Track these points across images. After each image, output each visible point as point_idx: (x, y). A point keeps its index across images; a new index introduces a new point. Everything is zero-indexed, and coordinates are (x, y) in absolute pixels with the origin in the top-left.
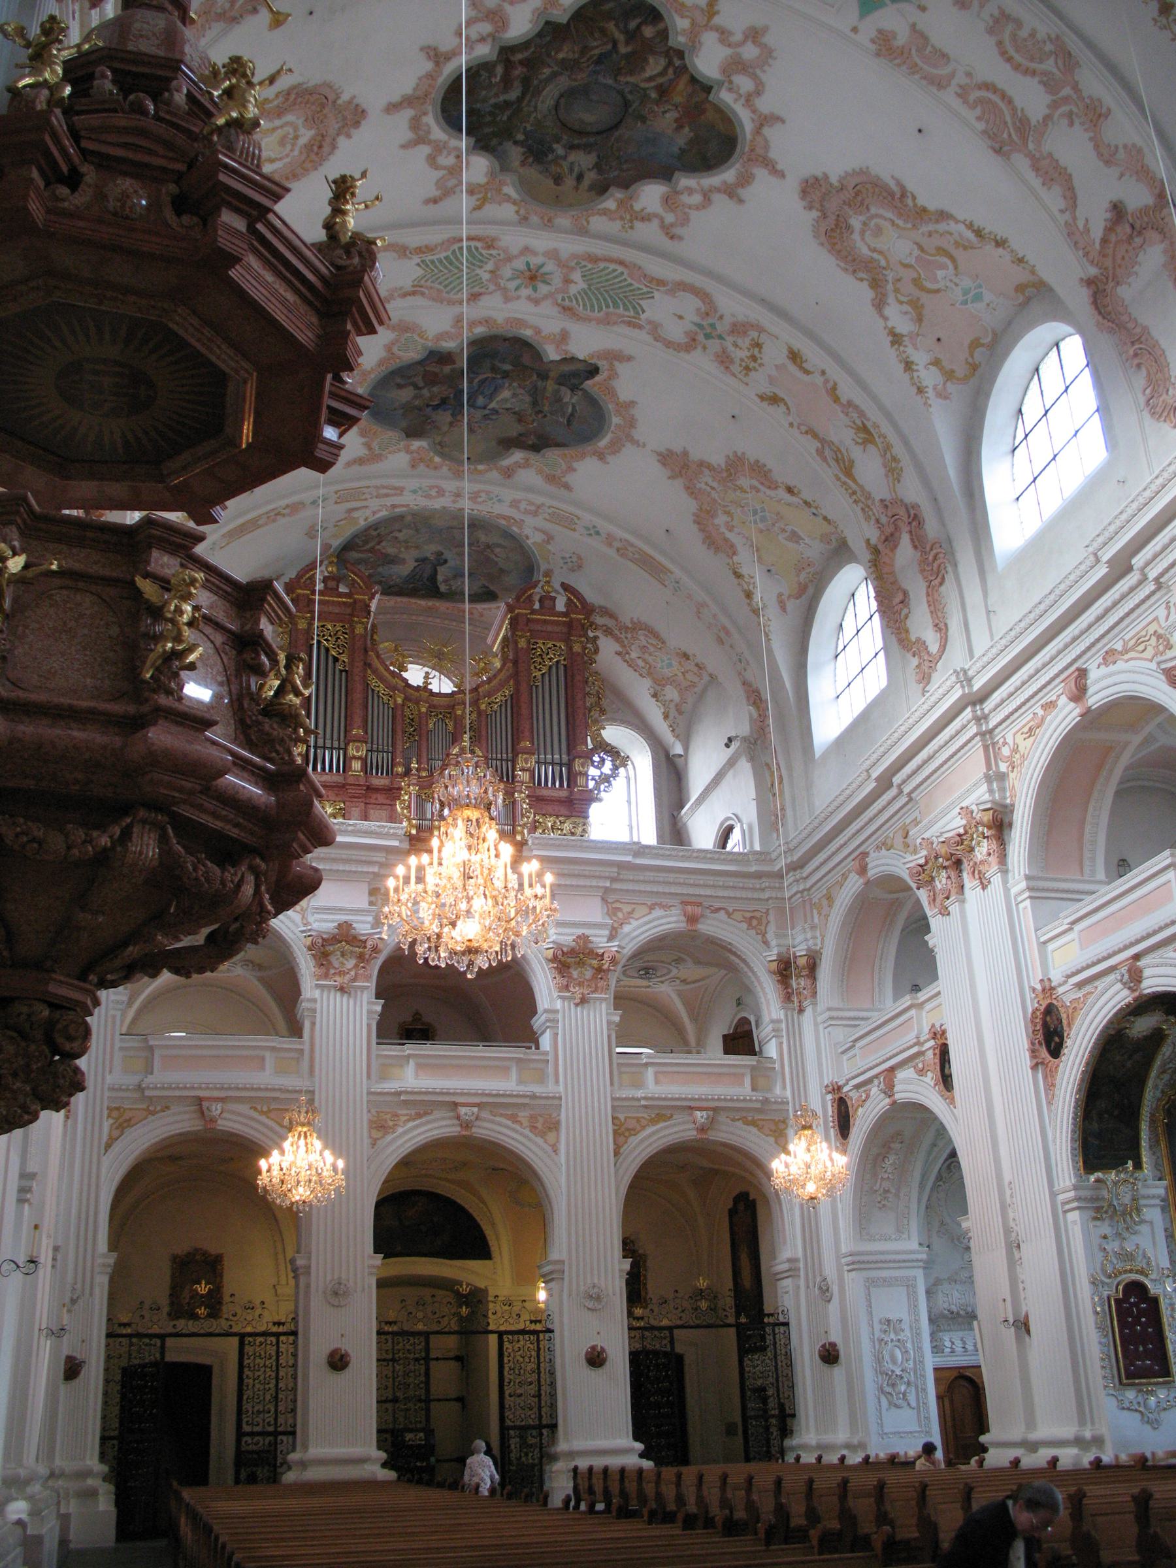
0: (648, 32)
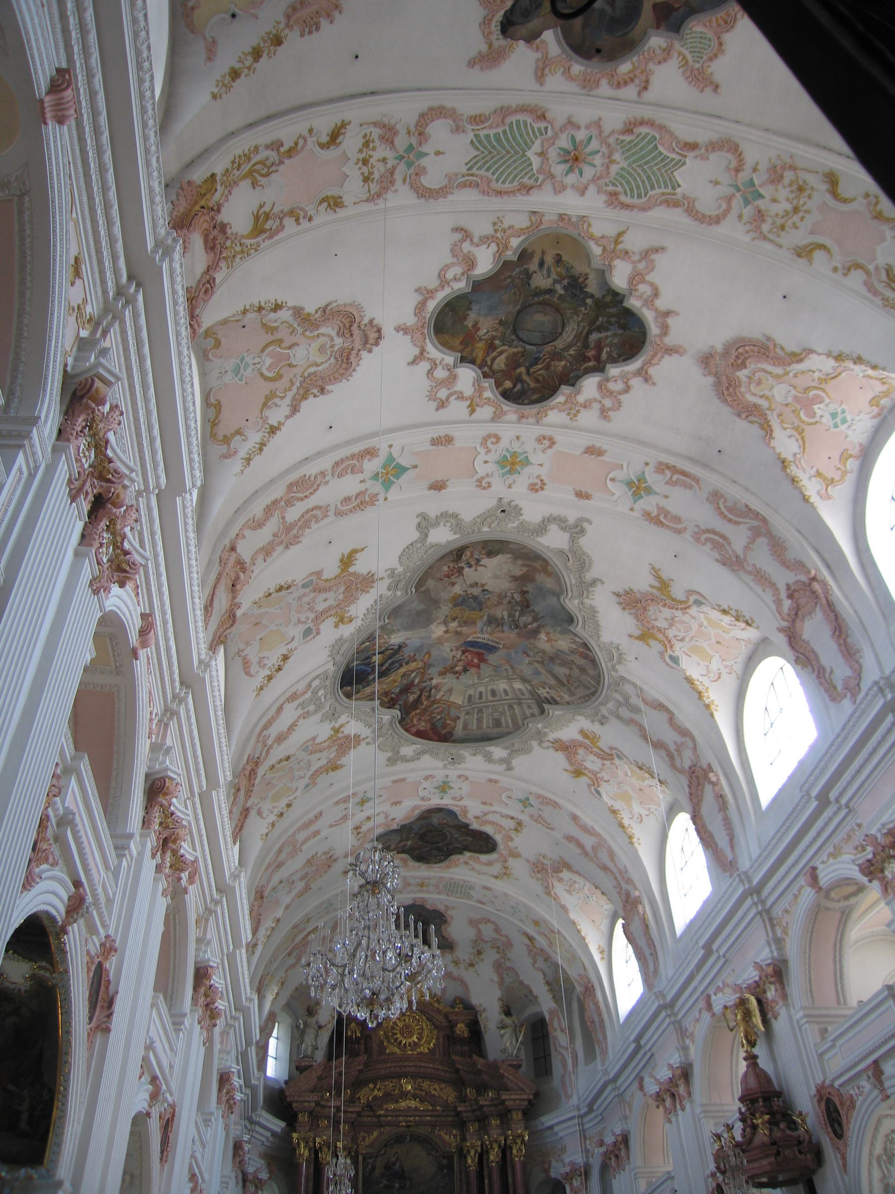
0: (508, 384)
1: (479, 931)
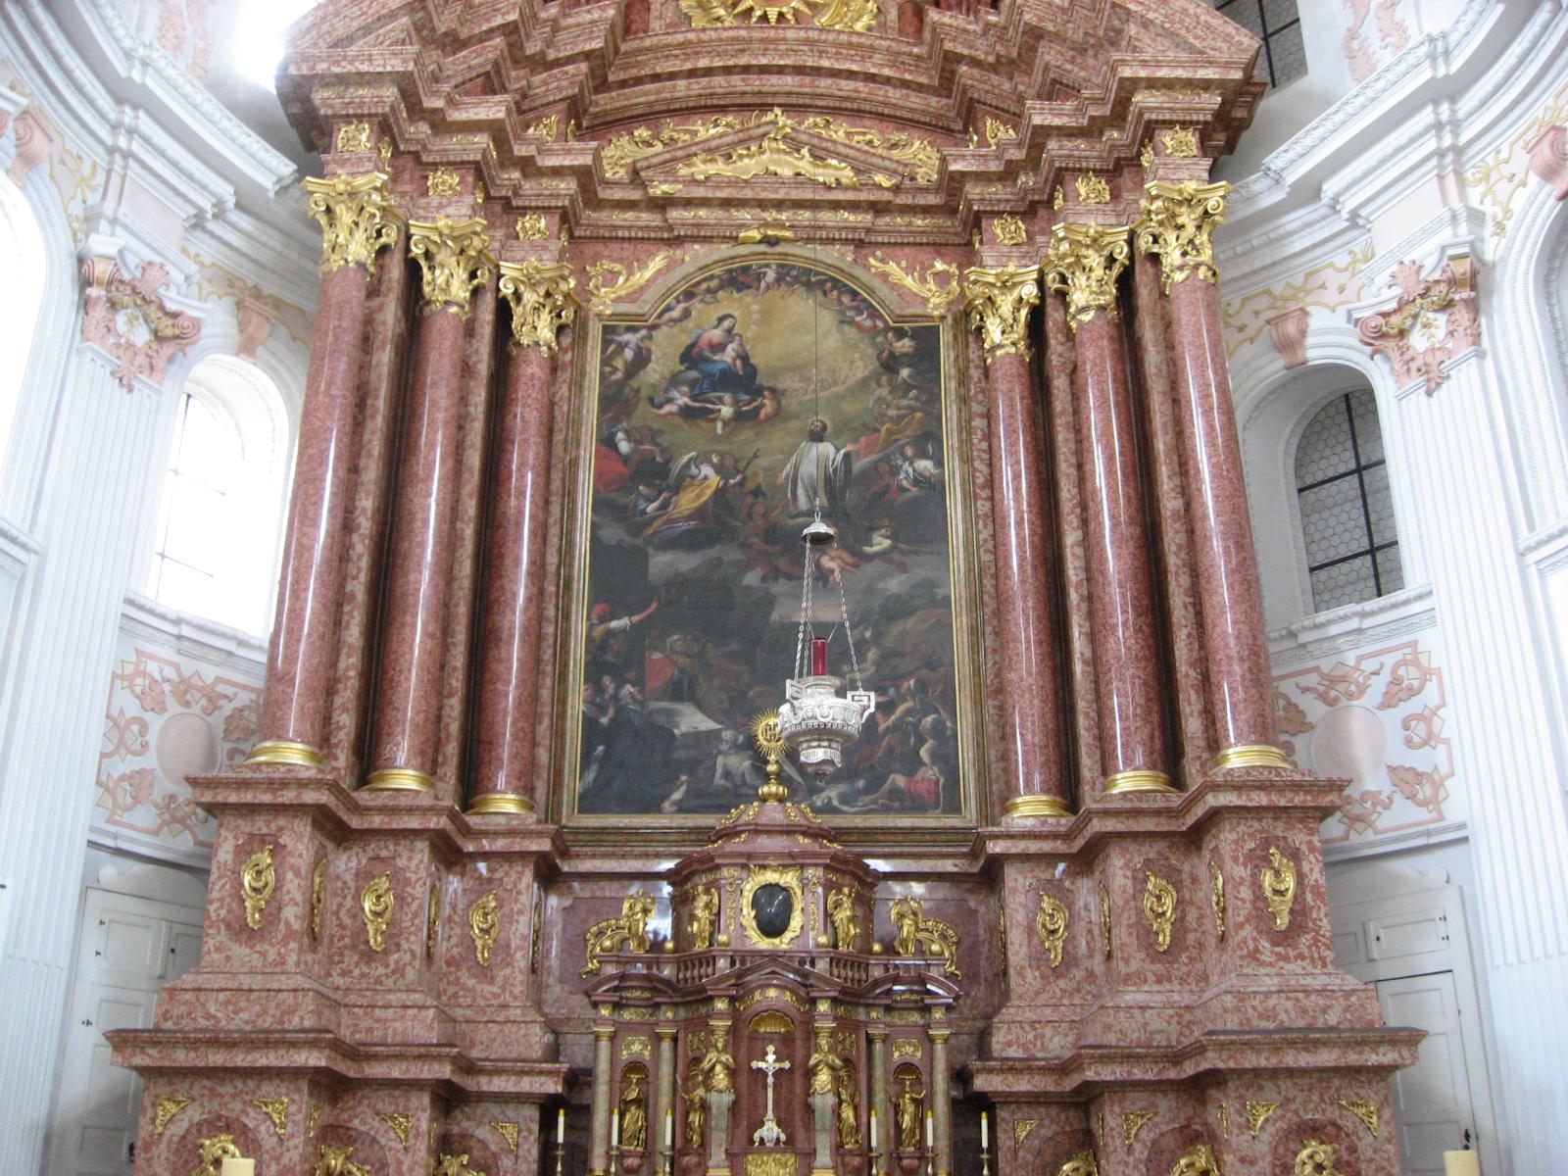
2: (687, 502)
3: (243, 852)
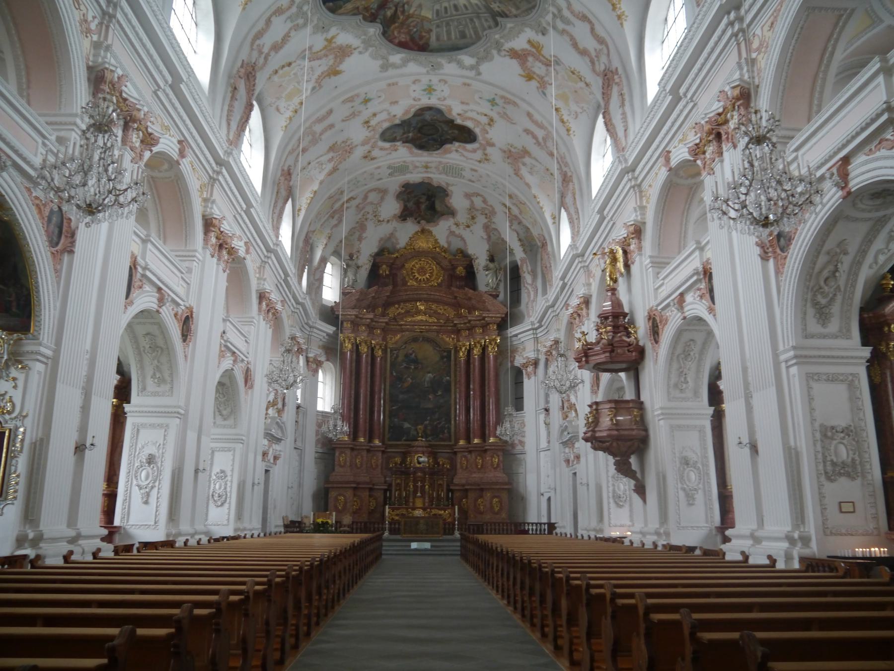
1: (472, 202)
2: (406, 385)
3: (340, 454)
